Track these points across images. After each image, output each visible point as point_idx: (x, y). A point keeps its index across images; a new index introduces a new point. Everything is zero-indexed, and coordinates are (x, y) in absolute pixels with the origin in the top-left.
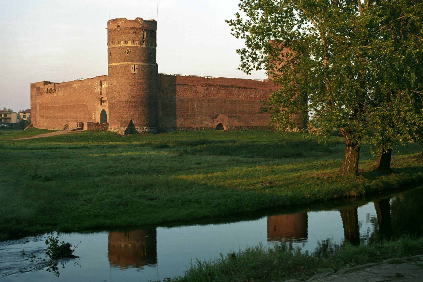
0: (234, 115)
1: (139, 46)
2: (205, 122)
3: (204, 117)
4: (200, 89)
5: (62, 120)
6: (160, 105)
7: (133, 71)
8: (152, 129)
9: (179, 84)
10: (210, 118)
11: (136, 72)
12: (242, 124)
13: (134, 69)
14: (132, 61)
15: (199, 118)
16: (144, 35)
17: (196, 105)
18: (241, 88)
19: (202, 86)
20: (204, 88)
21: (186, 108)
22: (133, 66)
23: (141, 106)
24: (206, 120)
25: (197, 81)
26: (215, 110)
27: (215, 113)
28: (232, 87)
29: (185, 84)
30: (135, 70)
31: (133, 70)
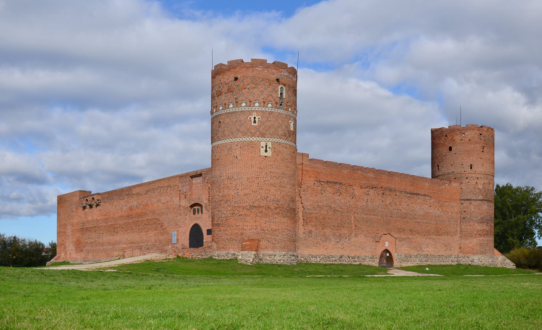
5: (112, 247)
6: (300, 215)
7: (263, 153)
8: (294, 256)
11: (269, 153)
13: (265, 149)
14: (263, 135)
17: (353, 218)
19: (361, 188)
21: (339, 222)
22: (263, 144)
30: (266, 151)
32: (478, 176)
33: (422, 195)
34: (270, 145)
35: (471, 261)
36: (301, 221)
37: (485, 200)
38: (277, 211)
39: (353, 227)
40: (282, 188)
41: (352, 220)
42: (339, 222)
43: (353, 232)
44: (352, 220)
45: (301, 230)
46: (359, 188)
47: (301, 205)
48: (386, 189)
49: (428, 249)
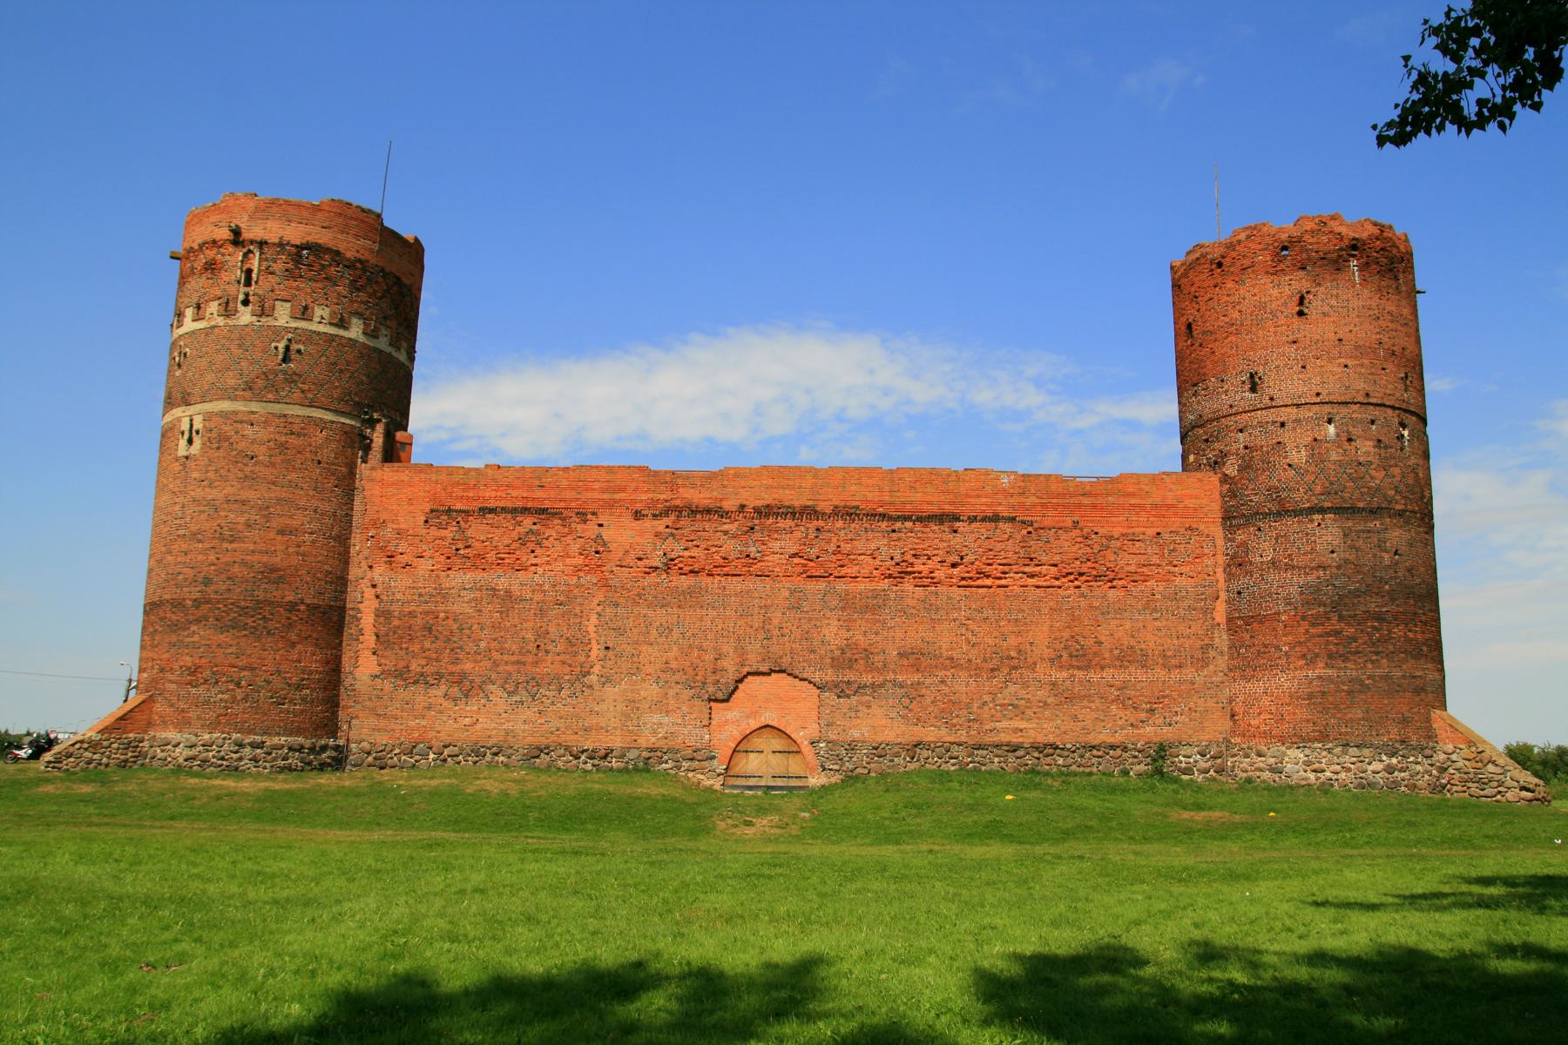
0: (867, 679)
1: (221, 321)
2: (656, 718)
3: (651, 690)
4: (622, 534)
6: (367, 620)
9: (492, 511)
10: (688, 693)
12: (930, 734)
13: (186, 436)
15: (611, 692)
16: (249, 272)
18: (920, 519)
19: (638, 515)
20: (648, 524)
23: (198, 621)
24: (660, 705)
25: (603, 491)
26: (728, 648)
27: (724, 663)
28: (848, 513)
29: (525, 510)
30: (190, 441)
31: (183, 443)
32: (1283, 414)
33: (972, 519)
34: (198, 425)
35: (1273, 770)
36: (369, 639)
37: (1322, 511)
38: (199, 613)
39: (594, 653)
40: (226, 545)
41: (591, 629)
42: (530, 636)
43: (596, 669)
44: (591, 629)
45: (363, 666)
46: (628, 521)
47: (369, 593)
48: (764, 512)
49: (1022, 725)
